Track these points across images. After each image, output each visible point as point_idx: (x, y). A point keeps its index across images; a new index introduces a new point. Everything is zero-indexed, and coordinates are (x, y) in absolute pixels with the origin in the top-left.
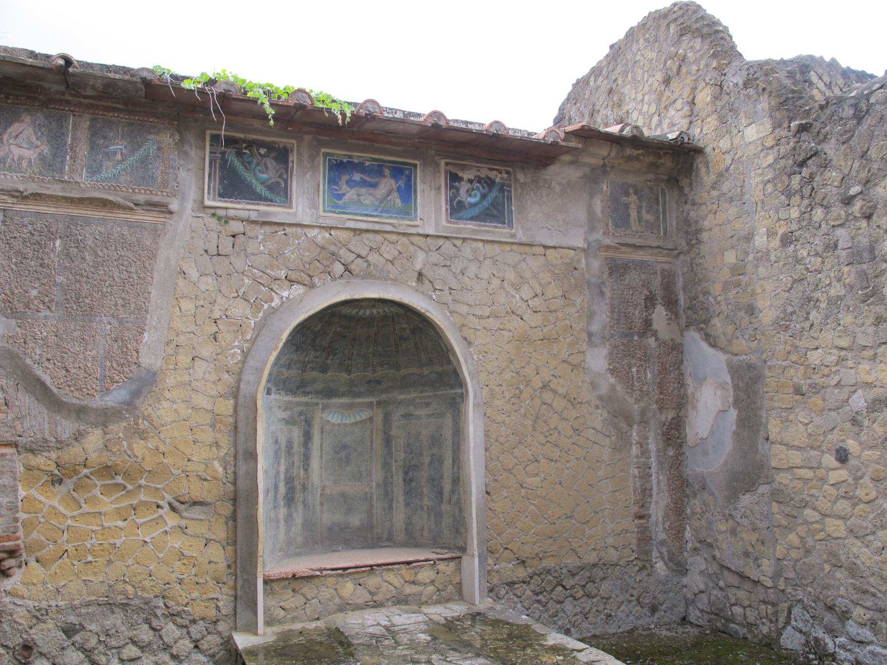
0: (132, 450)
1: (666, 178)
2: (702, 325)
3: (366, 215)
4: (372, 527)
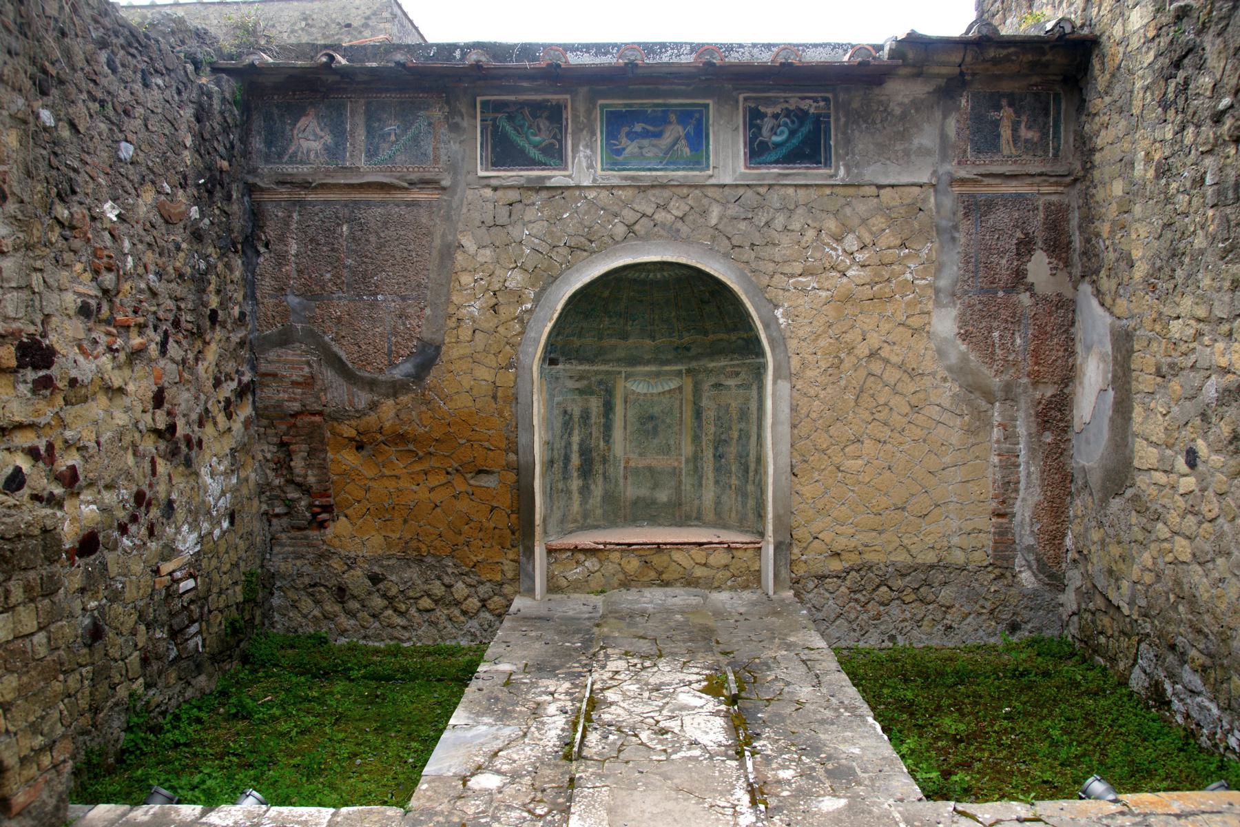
1: (1060, 78)
2: (1094, 277)
3: (650, 170)
4: (680, 505)
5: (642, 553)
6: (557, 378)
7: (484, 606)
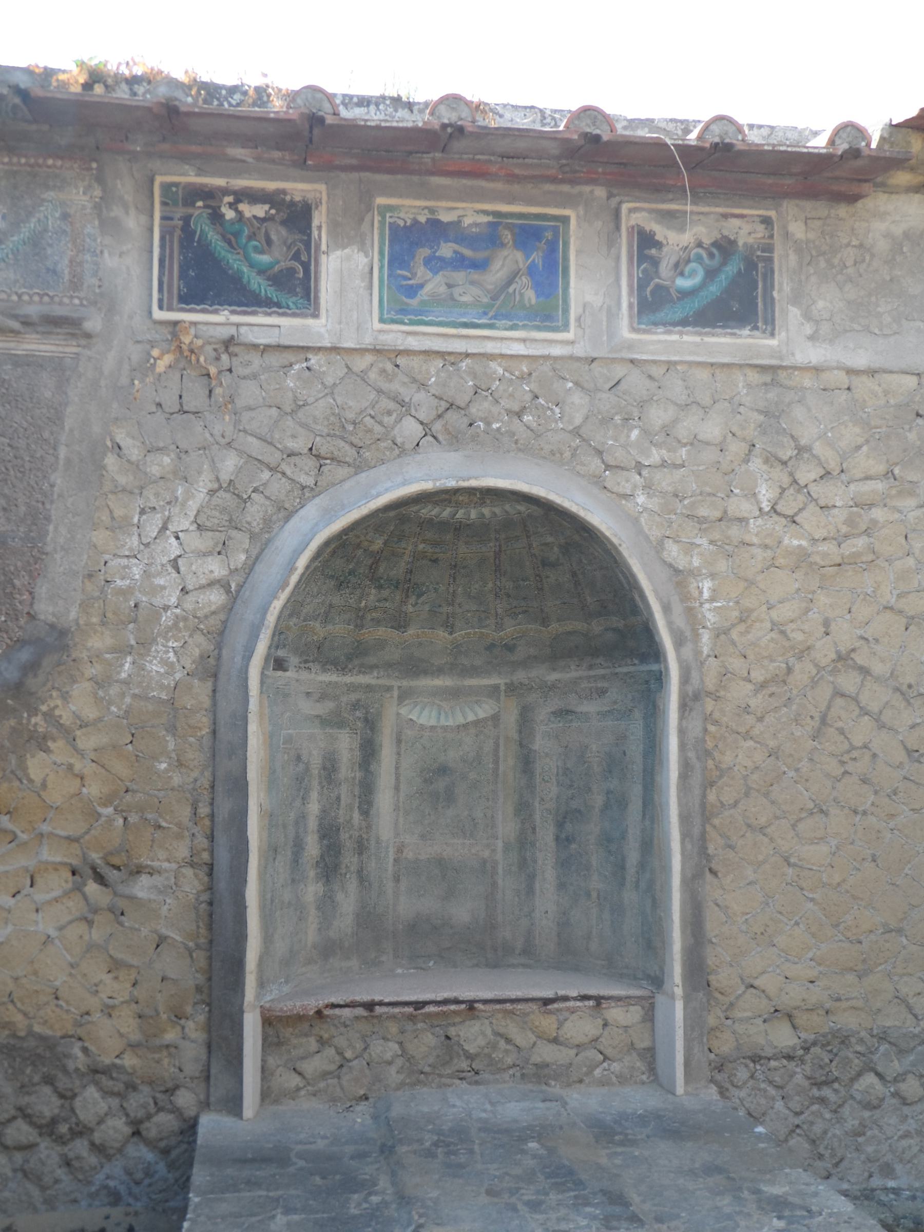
0: (25, 769)
3: (466, 325)
6: (286, 696)
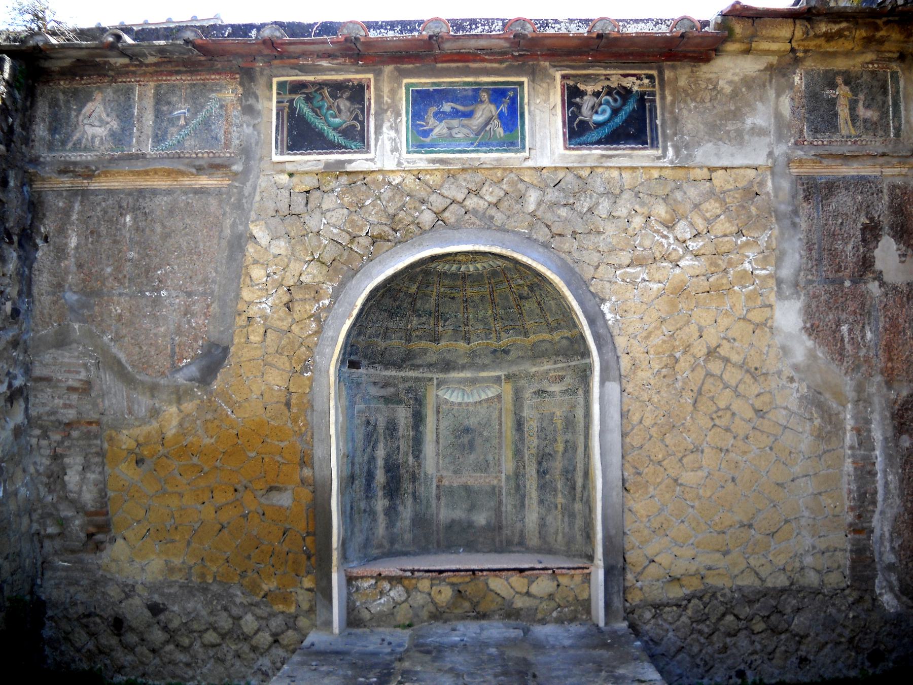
1: (896, 55)
3: (460, 152)
4: (500, 528)
5: (454, 580)
6: (359, 384)
7: (276, 641)
